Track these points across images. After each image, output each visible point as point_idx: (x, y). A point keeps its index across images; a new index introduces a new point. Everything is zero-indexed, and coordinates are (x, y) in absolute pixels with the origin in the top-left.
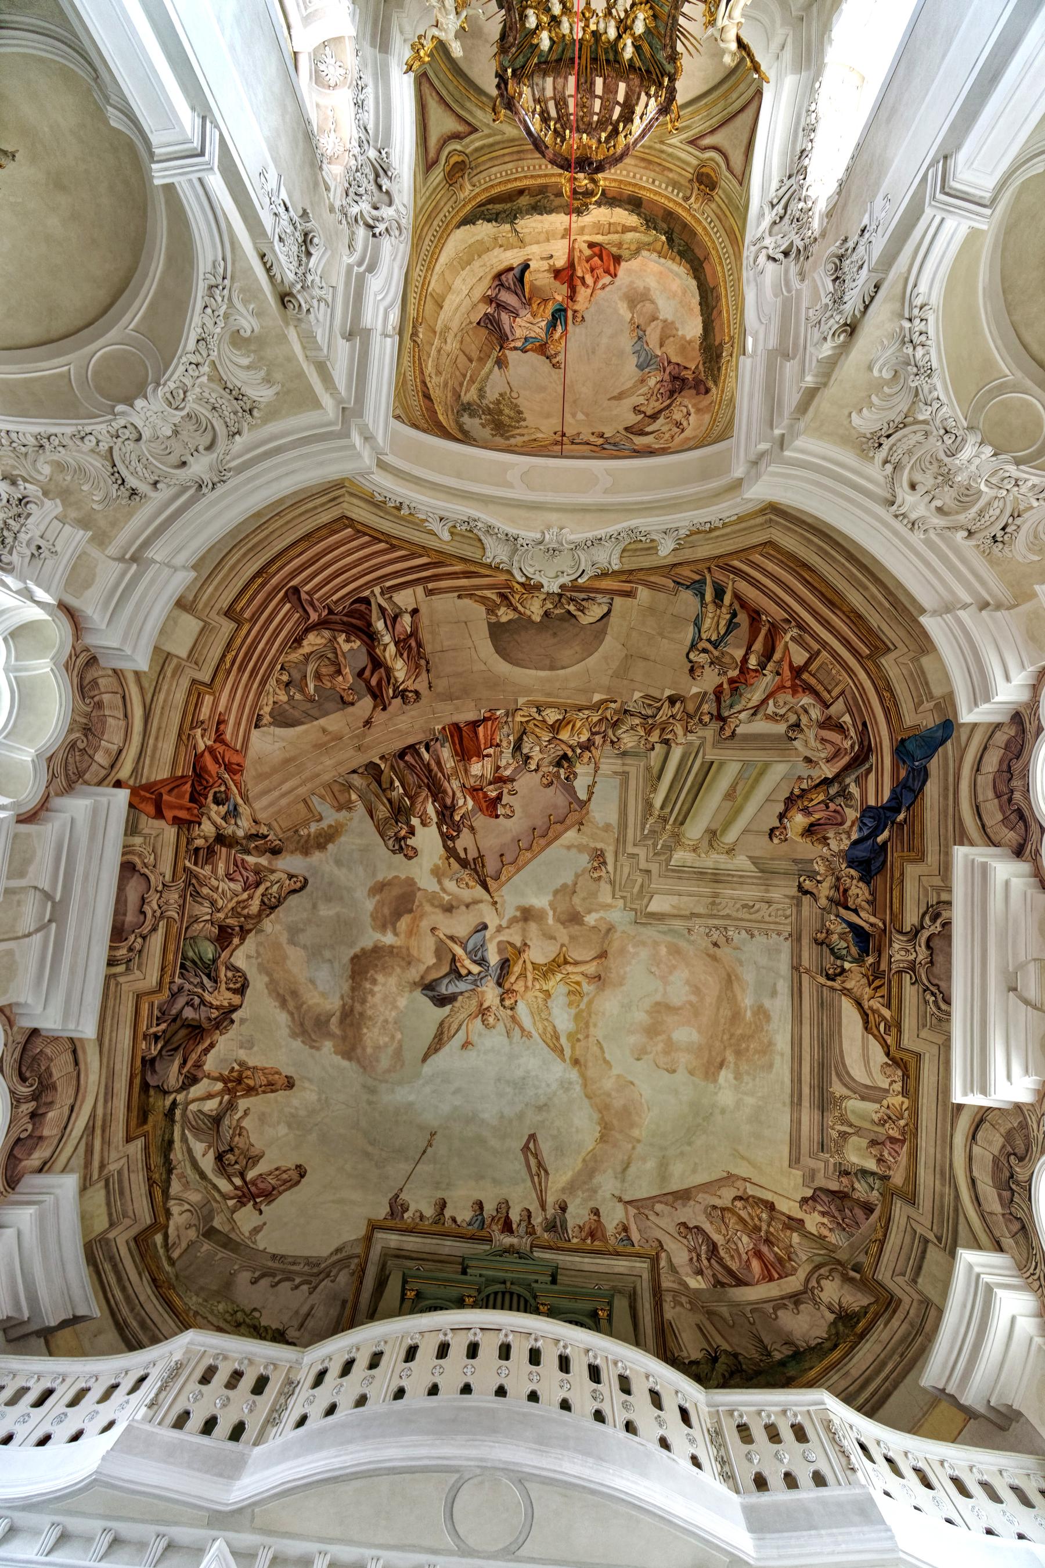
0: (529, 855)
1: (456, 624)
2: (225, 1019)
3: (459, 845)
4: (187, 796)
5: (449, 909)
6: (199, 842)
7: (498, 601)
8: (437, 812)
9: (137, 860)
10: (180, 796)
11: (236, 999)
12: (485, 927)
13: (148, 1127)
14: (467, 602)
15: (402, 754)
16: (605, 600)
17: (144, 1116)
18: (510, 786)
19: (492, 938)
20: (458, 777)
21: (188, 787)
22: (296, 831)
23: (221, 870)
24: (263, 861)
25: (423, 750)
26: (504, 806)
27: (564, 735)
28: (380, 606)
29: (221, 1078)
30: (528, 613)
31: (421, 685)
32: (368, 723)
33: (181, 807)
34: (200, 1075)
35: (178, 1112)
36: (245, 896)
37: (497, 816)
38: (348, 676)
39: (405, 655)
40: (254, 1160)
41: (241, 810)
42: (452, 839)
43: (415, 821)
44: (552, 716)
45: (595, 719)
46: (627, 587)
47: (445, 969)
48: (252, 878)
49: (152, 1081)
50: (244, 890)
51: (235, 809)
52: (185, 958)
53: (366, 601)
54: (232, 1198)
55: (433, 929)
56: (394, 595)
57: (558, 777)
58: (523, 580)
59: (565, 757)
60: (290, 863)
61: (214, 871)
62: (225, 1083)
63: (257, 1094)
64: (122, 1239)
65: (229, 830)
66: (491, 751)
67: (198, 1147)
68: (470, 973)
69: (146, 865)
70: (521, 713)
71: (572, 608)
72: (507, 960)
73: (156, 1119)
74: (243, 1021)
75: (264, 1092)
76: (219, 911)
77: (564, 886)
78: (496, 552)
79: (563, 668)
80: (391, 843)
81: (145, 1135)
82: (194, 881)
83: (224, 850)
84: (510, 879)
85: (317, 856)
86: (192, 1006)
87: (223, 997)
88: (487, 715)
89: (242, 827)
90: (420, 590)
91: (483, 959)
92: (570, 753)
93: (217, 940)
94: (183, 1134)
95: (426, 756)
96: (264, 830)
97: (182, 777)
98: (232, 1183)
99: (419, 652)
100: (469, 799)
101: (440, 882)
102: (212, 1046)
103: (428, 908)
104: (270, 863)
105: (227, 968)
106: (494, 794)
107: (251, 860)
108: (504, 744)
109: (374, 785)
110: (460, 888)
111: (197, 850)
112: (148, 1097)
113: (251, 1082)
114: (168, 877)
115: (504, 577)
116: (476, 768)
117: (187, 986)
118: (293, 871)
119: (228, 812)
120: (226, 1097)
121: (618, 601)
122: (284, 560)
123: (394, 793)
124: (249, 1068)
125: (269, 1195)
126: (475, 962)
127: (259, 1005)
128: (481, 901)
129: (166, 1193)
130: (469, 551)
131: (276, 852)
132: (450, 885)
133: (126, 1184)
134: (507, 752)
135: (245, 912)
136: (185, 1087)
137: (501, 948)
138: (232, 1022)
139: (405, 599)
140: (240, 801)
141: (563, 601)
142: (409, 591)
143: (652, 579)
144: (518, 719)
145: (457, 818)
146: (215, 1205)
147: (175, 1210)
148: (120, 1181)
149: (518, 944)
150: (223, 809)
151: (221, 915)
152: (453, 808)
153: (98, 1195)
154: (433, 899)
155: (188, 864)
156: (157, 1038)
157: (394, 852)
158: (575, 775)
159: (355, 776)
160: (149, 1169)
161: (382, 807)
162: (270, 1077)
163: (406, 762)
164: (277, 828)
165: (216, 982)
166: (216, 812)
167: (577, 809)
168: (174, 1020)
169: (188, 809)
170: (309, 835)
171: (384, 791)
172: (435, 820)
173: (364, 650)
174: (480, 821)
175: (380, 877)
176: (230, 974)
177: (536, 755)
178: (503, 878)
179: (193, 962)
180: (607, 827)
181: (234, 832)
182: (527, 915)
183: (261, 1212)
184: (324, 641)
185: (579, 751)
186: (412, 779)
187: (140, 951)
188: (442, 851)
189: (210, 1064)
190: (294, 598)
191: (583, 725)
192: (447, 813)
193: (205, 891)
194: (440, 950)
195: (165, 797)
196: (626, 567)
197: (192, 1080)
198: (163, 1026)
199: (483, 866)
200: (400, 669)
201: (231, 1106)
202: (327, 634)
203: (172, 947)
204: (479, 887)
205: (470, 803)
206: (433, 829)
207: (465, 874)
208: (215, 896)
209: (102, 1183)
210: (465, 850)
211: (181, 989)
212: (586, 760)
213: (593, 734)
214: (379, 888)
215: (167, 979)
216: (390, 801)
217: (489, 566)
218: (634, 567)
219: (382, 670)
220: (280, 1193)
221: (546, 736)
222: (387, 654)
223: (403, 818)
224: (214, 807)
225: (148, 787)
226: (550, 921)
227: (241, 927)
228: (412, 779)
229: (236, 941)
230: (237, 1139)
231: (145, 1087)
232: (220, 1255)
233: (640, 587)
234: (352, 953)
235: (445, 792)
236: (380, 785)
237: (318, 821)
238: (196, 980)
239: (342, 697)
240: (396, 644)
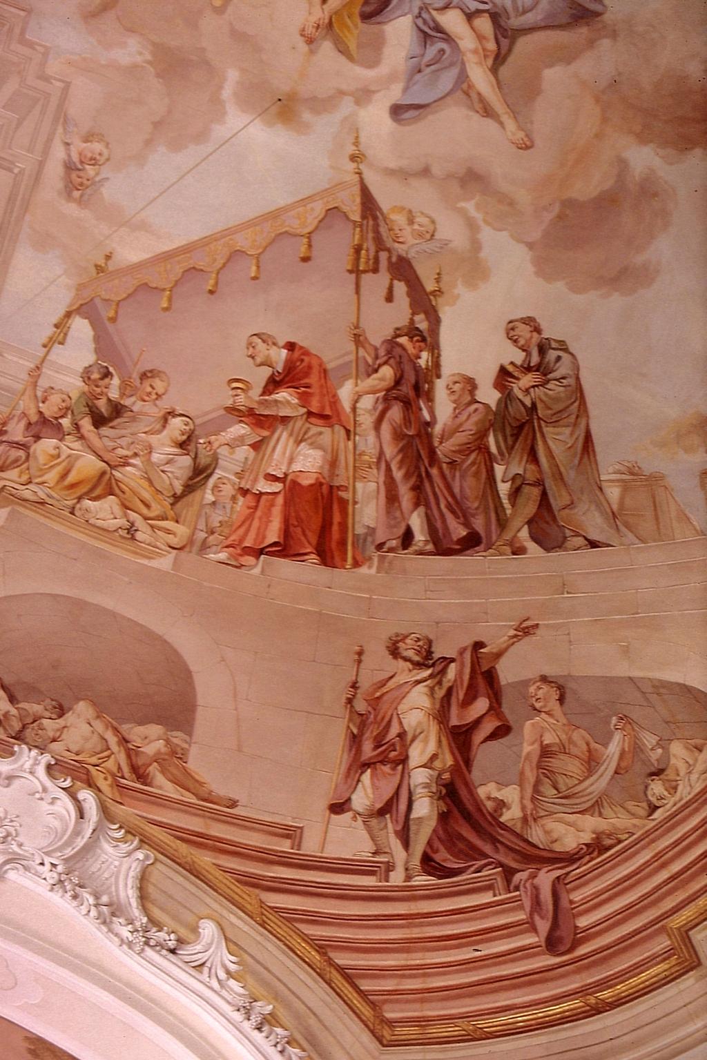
0: (241, 241)
1: (267, 749)
3: (400, 312)
5: (472, 179)
8: (430, 398)
12: (397, 111)
15: (472, 542)
18: (242, 401)
19: (392, 78)
20: (358, 455)
25: (420, 536)
26: (267, 363)
27: (88, 465)
28: (406, 844)
31: (378, 664)
32: (525, 631)
37: (291, 346)
38: (531, 734)
39: (394, 730)
42: (413, 332)
43: (489, 396)
44: (105, 511)
45: (13, 474)
47: (524, 45)
53: (429, 864)
55: (527, 147)
56: (366, 856)
57: (125, 386)
59: (99, 421)
66: (264, 486)
68: (470, 16)
70: (174, 541)
72: (366, 17)
77: (176, 145)
79: (55, 597)
80: (563, 369)
84: (304, 201)
88: (250, 560)
91: (425, 38)
92: (86, 424)
95: (417, 522)
99: (362, 726)
100: (347, 405)
101: (476, 246)
103: (523, 197)
106: (283, 395)
108: (228, 490)
109: (558, 500)
110: (427, 218)
116: (308, 462)
122: (540, 1013)
123: (517, 468)
126: (448, 38)
128: (391, 172)
132: (451, 231)
134: (226, 472)
137: (372, 53)
142: (334, 851)
144: (182, 530)
145: (387, 372)
149: (327, 46)
152: (390, 396)
154: (505, 209)
157: (563, 347)
158: (86, 376)
159: (594, 536)
163: (467, 524)
167: (102, 301)
171: (539, 483)
172: (440, 387)
173: (476, 775)
174: (332, 349)
177: (163, 449)
178: (319, 208)
180: (43, 242)
182: (285, 108)
184: (550, 824)
185: (66, 422)
186: (467, 486)
188: (447, 315)
190: (565, 932)
191: (43, 472)
192: (406, 389)
194: (522, 96)
199: (358, 250)
200: (415, 709)
202: (536, 835)
204: (384, 201)
205: (345, 393)
206: (452, 363)
207: (409, 244)
210: (389, 298)
212: (55, 399)
213: (24, 446)
216: (533, 457)
219: (454, 721)
221: (130, 475)
222: (432, 747)
223: (515, 411)
226: (233, 75)
228: (467, 486)
235: (398, 435)
236: (544, 495)
239: (561, 700)
240: (404, 760)
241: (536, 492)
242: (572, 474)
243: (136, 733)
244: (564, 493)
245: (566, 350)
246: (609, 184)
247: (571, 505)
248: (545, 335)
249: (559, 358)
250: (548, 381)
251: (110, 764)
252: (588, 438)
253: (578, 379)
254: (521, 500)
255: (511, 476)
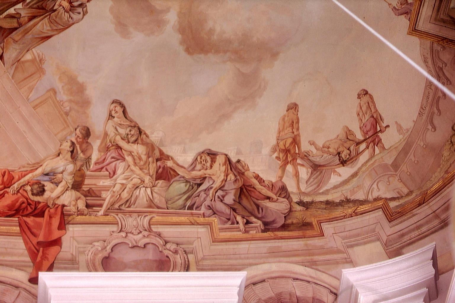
2: (236, 168)
4: (39, 219)
6: (81, 205)
9: (100, 256)
10: (39, 226)
11: (220, 159)
13: (314, 222)
17: (306, 225)
21: (30, 220)
22: (67, 114)
23: (107, 182)
24: (96, 144)
29: (283, 167)
33: (49, 224)
34: (280, 185)
35: (306, 199)
36: (129, 159)
40: (349, 133)
41: (48, 170)
48: (113, 153)
49: (281, 222)
50: (124, 159)
51: (47, 175)
52: (184, 207)
54: (374, 150)
60: (98, 118)
61: (106, 189)
62: (288, 163)
63: (299, 135)
64: (389, 230)
65: (68, 179)
67: (334, 180)
69: (104, 248)
73: (311, 217)
74: (239, 153)
75: (298, 129)
76: (143, 181)
80: (75, 16)
81: (320, 223)
82: (117, 206)
83: (87, 182)
85: (91, 92)
86: (223, 197)
87: (218, 171)
89: (65, 166)
93: (169, 180)
94: (323, 193)
96: (67, 146)
97: (20, 226)
98: (363, 151)
102: (257, 177)
104: (98, 138)
105: (193, 169)
107: (95, 156)
111: (88, 206)
112: (292, 224)
113: (289, 141)
114: (114, 228)
117: (208, 202)
118: (106, 115)
119: (51, 181)
120: (299, 161)
123: (23, 13)
124: (278, 144)
125: (376, 120)
127: (228, 140)
129: (362, 202)
131: (87, 133)
133: (352, 233)
135: (144, 157)
136: (288, 197)
138: (239, 161)
140: (39, 171)
146: (376, 164)
147: (375, 194)
148: (350, 237)
150: (48, 186)
151: (147, 179)
153: (358, 252)
155: (101, 213)
156: (248, 222)
160: (344, 217)
161: (39, 27)
162: (287, 124)
164: (64, 133)
165: (205, 178)
166: (52, 193)
168: (234, 210)
169: (50, 217)
170: (70, 101)
171: (20, 25)
175: (111, 27)
176: (199, 167)
179: (187, 199)
181: (70, 174)
183: (388, 126)
187: (177, 244)
189: (270, 176)
193: (125, 195)
195: (41, 238)
197: (283, 191)
198: (239, 218)
201: (306, 156)
203: (175, 219)
208: (129, 186)
209: (350, 251)
211: (209, 207)
214: (122, 27)
215: (202, 220)
216: (31, 19)
220: (377, 111)
224: (47, 194)
225: (33, 255)
227: (157, 160)
229: (169, 164)
230: (331, 150)
231: (284, 227)
232: (412, 157)
234: (183, 53)
236: (16, 29)
237: (55, 93)
238: (203, 195)
241: (16, 25)
242: (30, 37)
244: (20, 36)
245: (84, 15)
246: (158, 7)
247: (16, 42)
248: (88, 4)
249: (79, 13)
250: (68, 12)
252: (49, 37)
253: (73, 24)
254: (9, 20)
255: (19, 11)
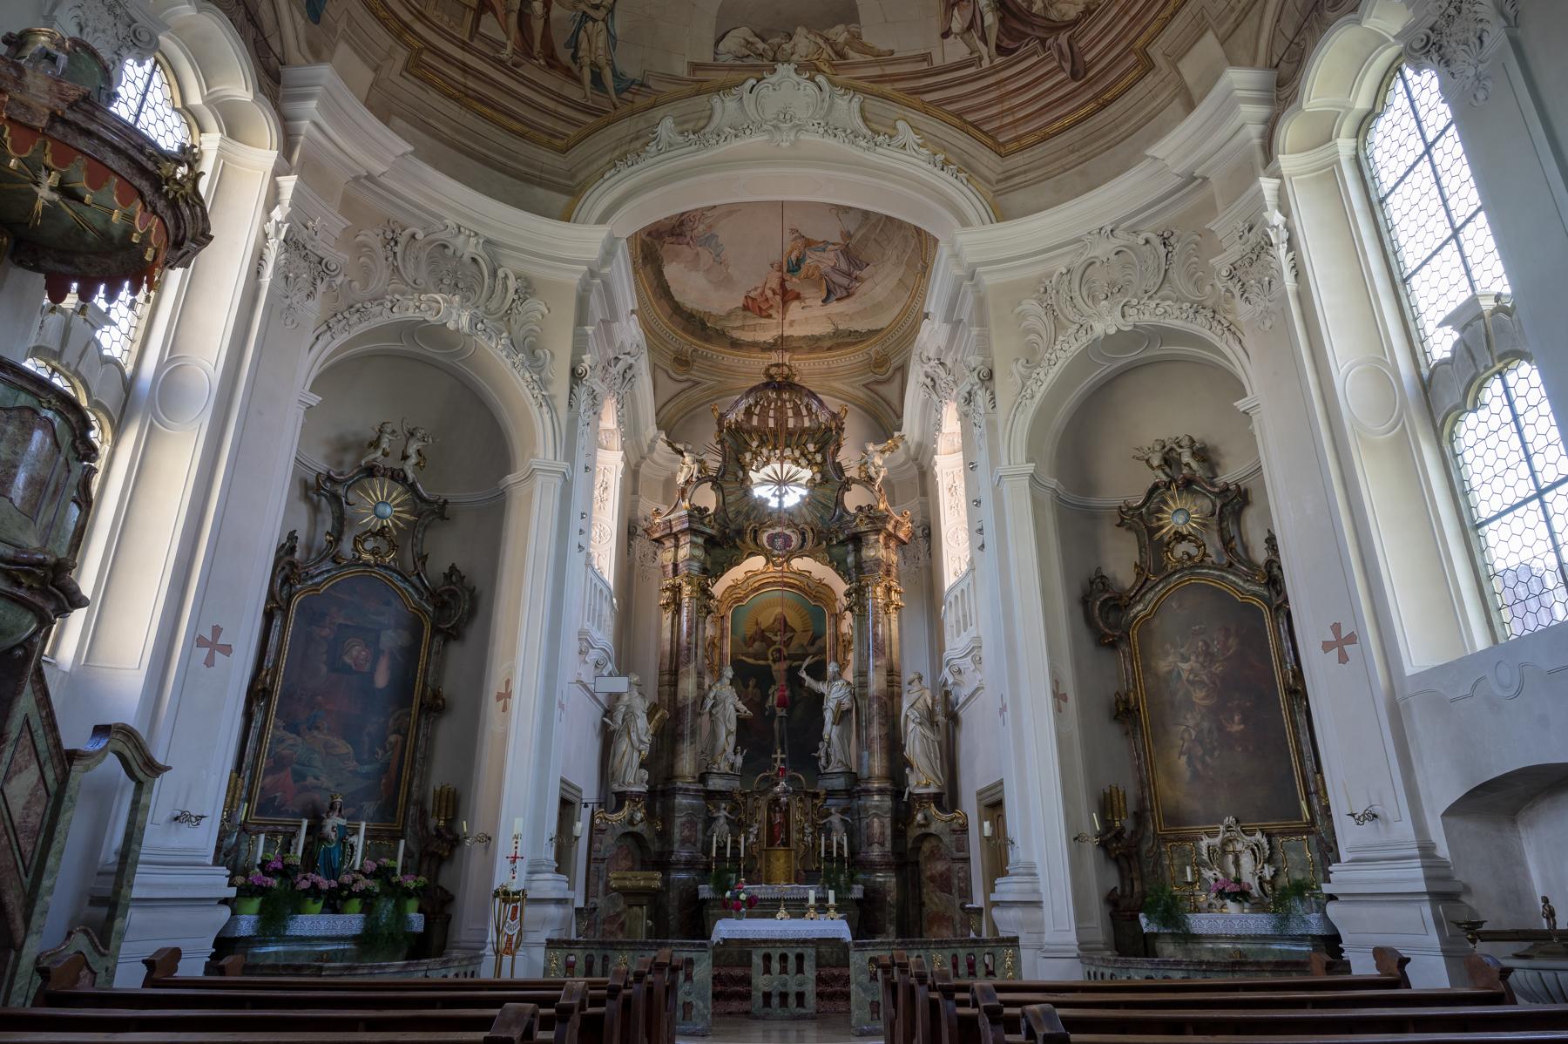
7: (847, 49)
14: (883, 47)
16: (722, 58)
30: (811, 37)
46: (700, 75)
58: (820, 78)
71: (761, 46)
78: (847, 108)
90: (938, 61)
115: (841, 78)
121: (707, 58)
130: (875, 106)
139: (956, 50)
141: (771, 54)
142: (949, 60)
143: (674, 88)
196: (704, 98)
217: (856, 90)
218: (697, 99)
233: (685, 75)
243: (831, 33)
251: (825, 55)
